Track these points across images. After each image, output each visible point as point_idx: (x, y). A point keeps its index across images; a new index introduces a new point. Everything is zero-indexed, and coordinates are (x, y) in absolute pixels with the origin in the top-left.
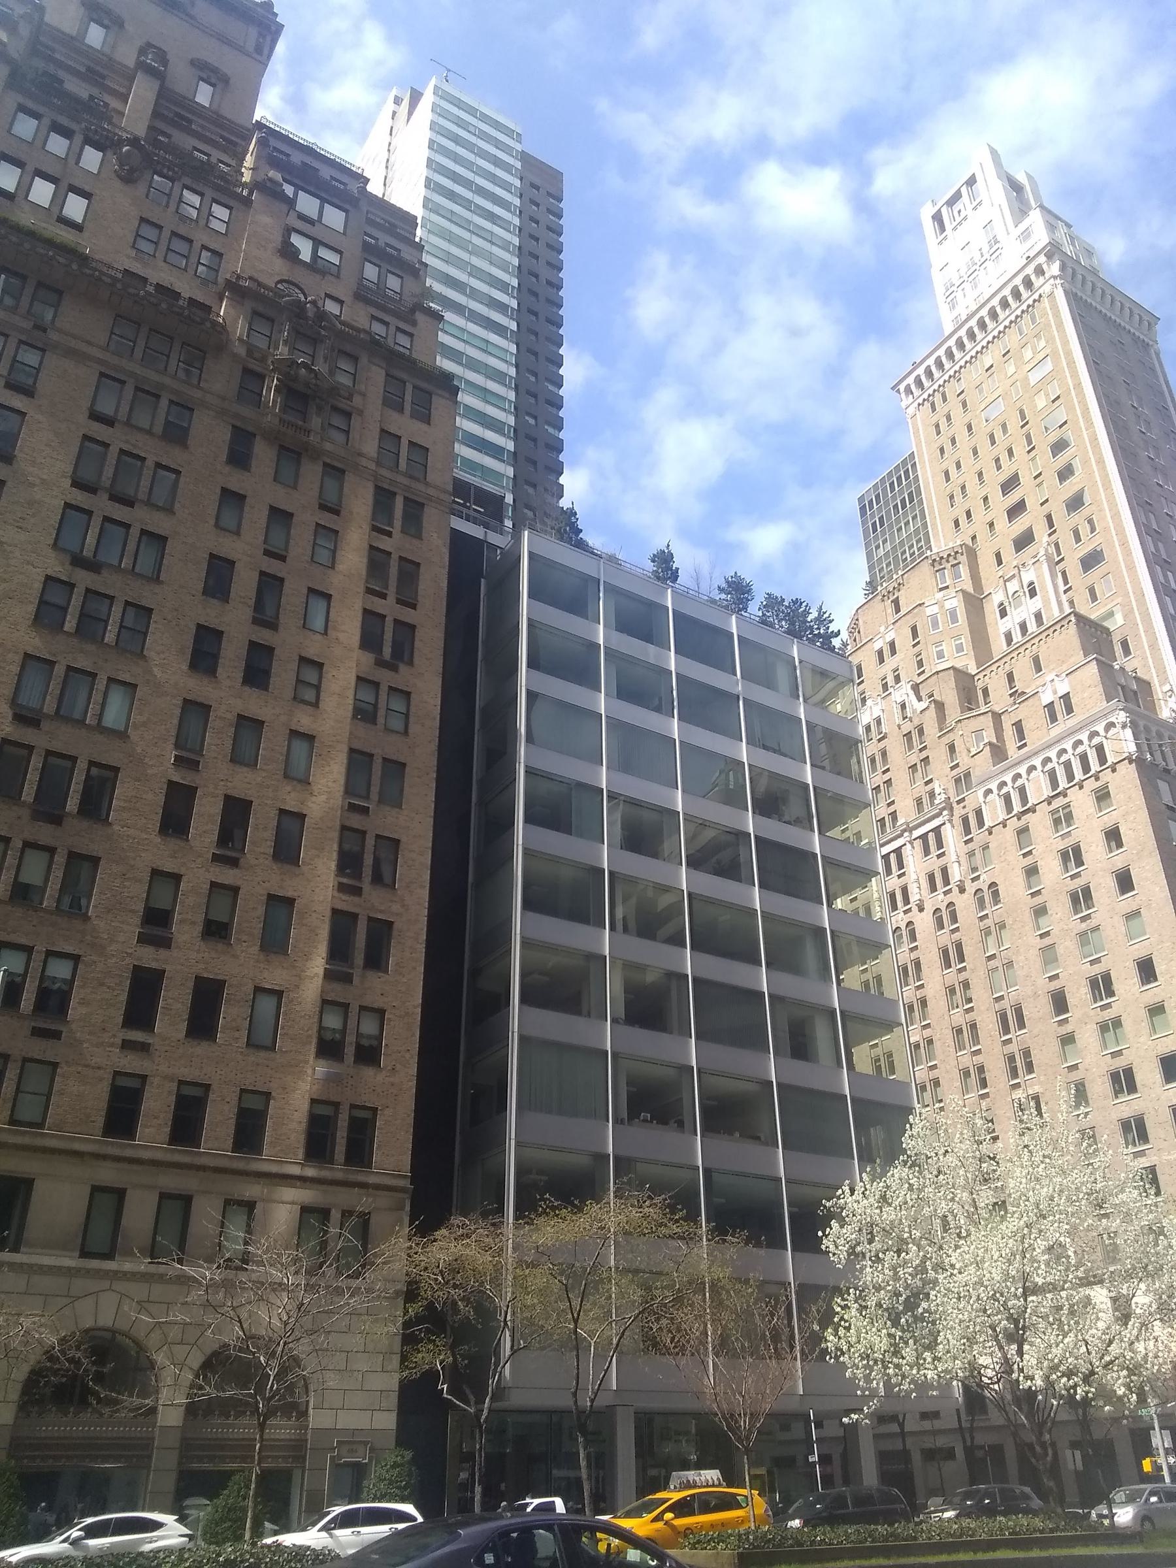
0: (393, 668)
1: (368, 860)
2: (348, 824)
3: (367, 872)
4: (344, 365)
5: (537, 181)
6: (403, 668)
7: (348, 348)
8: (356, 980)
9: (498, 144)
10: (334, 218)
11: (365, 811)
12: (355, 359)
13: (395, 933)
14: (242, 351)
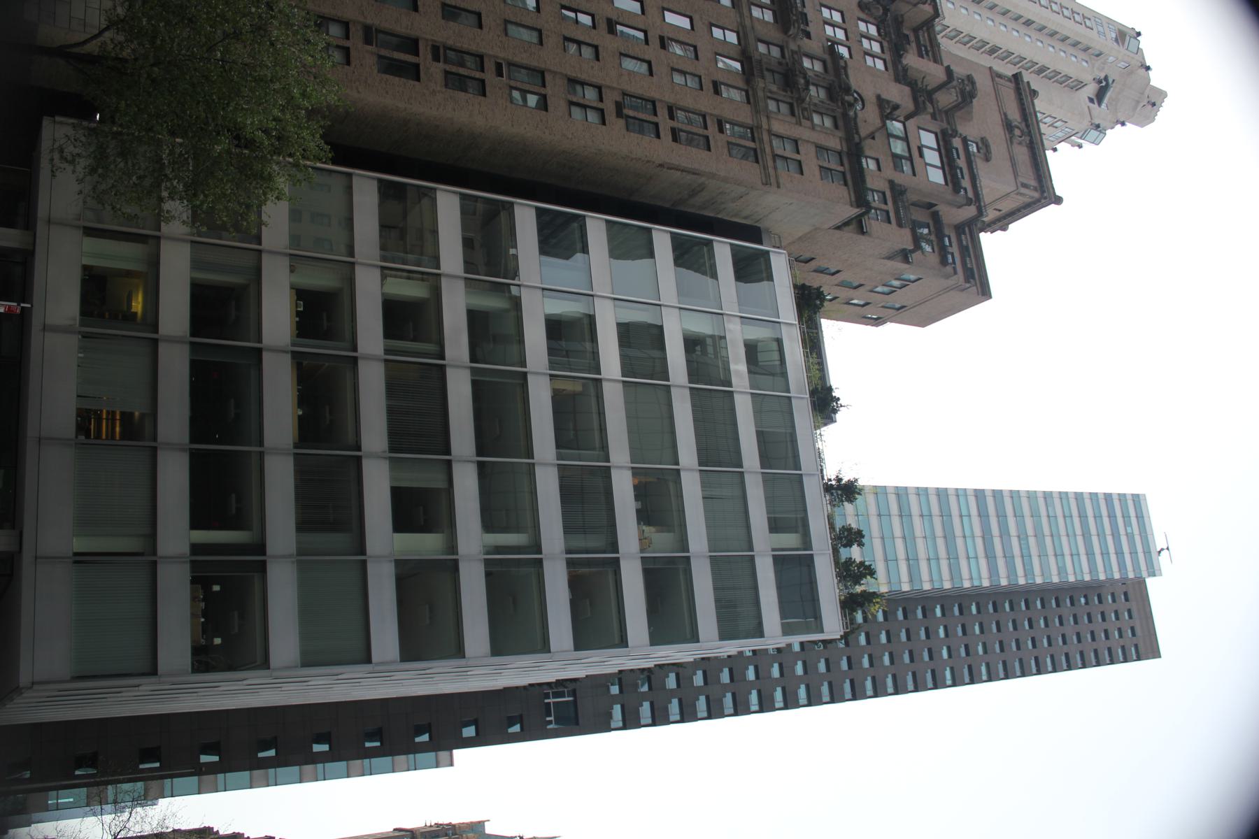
0: (619, 114)
1: (462, 71)
2: (486, 60)
3: (454, 69)
4: (828, 122)
5: (1135, 614)
6: (621, 122)
7: (840, 123)
8: (369, 48)
9: (1133, 553)
10: (936, 176)
11: (500, 74)
12: (836, 126)
13: (412, 82)
14: (793, 46)
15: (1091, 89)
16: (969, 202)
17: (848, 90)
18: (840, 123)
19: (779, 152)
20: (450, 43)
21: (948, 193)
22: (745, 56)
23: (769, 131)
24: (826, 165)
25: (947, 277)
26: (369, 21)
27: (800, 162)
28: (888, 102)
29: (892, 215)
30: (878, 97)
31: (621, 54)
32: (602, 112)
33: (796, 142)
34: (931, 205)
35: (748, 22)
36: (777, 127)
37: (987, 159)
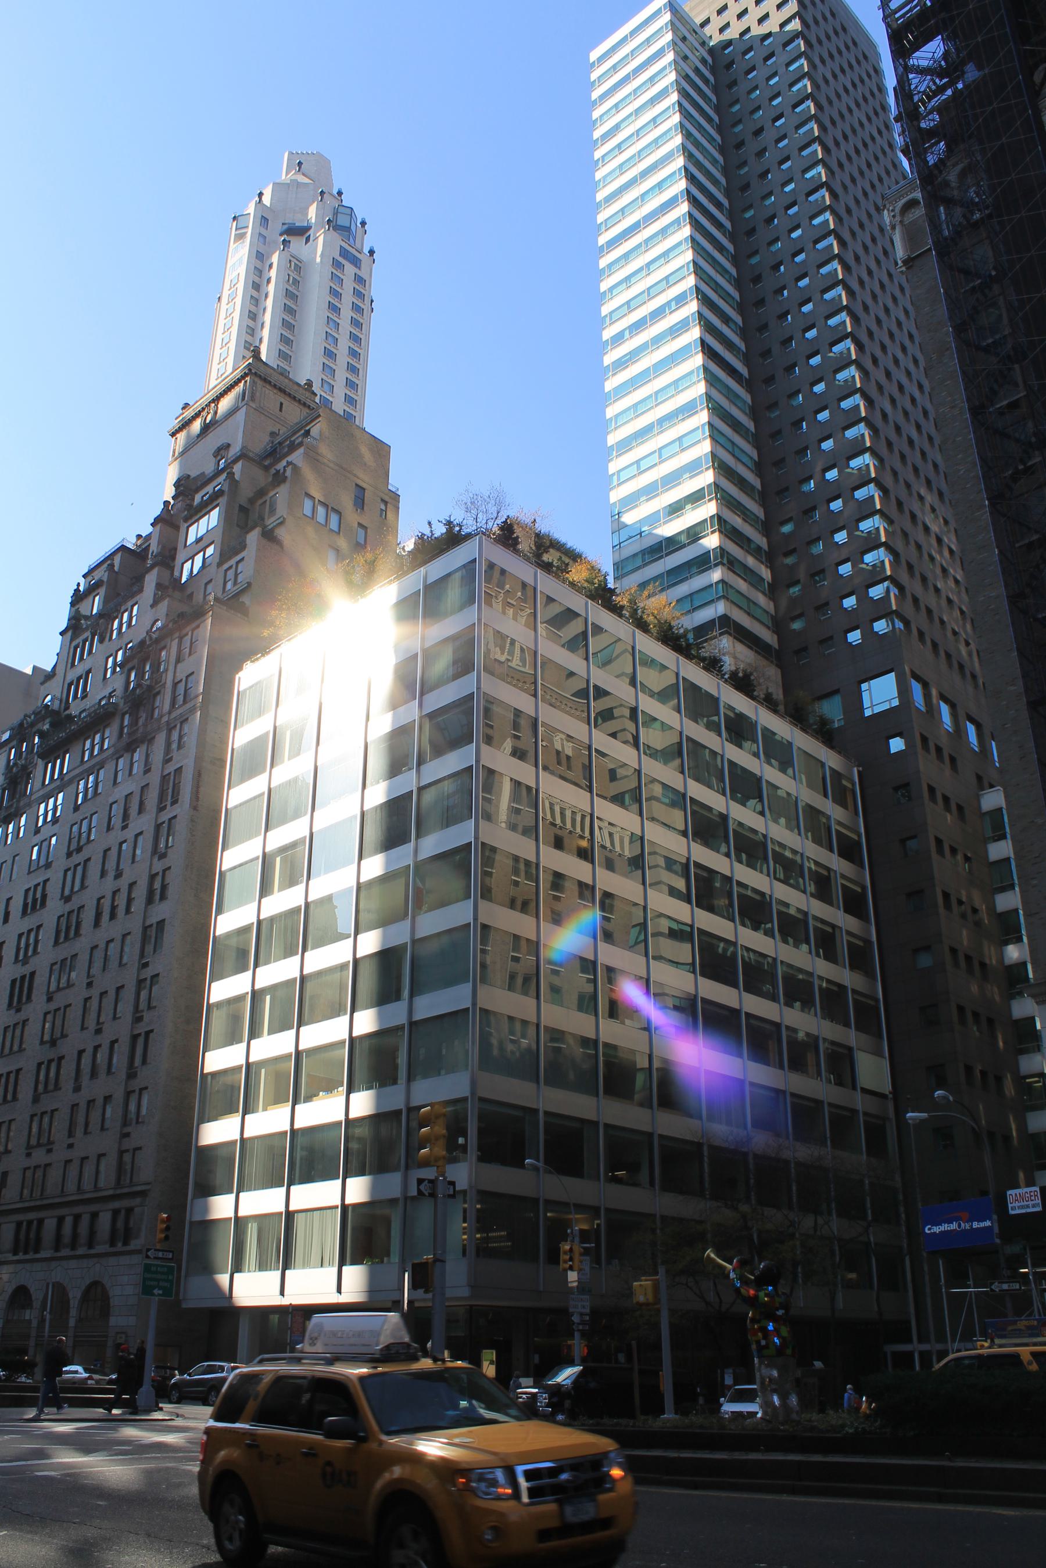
0: (163, 856)
4: (163, 653)
15: (297, 244)
16: (231, 475)
17: (142, 643)
18: (162, 644)
19: (181, 698)
20: (131, 1008)
21: (223, 500)
22: (130, 748)
23: (170, 713)
24: (187, 650)
25: (296, 469)
26: (124, 1077)
27: (187, 677)
28: (155, 595)
29: (238, 558)
30: (152, 606)
31: (133, 862)
32: (164, 871)
33: (175, 685)
34: (242, 509)
35: (110, 752)
36: (167, 707)
37: (228, 446)
